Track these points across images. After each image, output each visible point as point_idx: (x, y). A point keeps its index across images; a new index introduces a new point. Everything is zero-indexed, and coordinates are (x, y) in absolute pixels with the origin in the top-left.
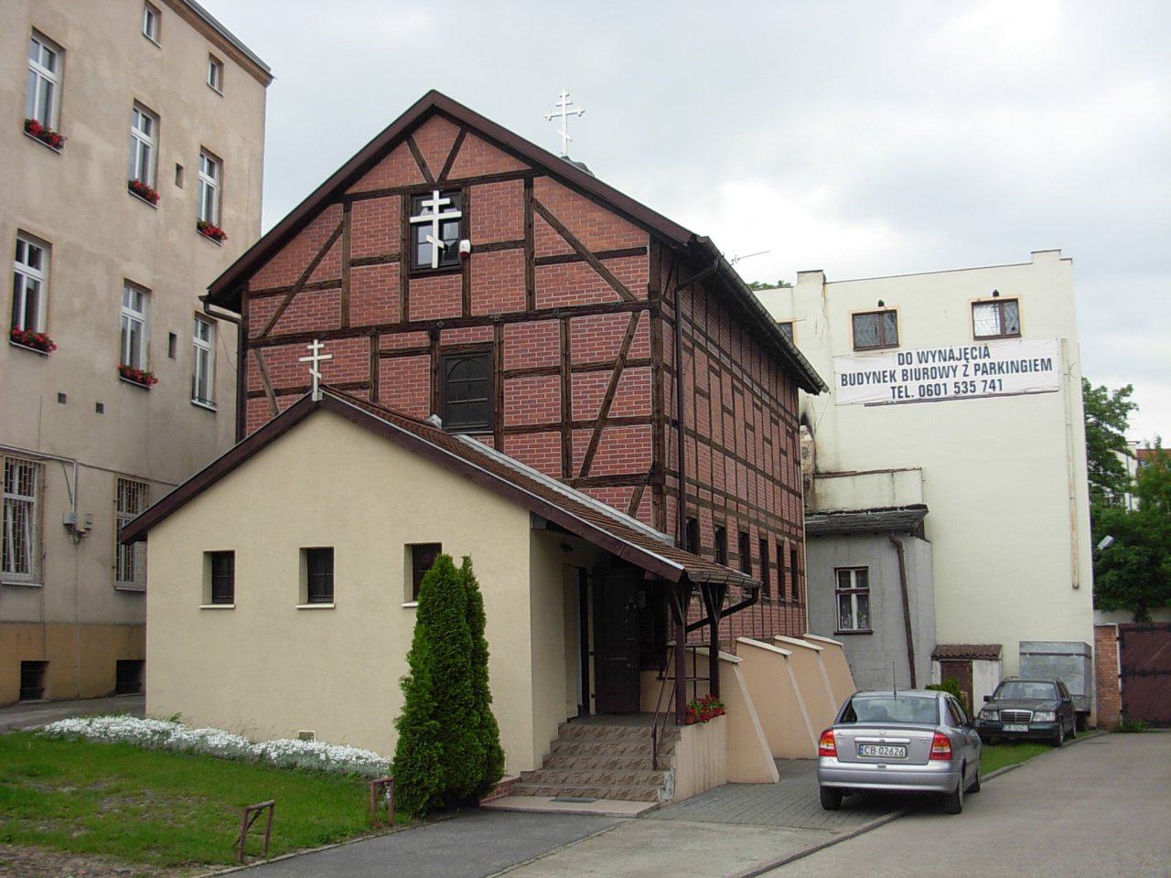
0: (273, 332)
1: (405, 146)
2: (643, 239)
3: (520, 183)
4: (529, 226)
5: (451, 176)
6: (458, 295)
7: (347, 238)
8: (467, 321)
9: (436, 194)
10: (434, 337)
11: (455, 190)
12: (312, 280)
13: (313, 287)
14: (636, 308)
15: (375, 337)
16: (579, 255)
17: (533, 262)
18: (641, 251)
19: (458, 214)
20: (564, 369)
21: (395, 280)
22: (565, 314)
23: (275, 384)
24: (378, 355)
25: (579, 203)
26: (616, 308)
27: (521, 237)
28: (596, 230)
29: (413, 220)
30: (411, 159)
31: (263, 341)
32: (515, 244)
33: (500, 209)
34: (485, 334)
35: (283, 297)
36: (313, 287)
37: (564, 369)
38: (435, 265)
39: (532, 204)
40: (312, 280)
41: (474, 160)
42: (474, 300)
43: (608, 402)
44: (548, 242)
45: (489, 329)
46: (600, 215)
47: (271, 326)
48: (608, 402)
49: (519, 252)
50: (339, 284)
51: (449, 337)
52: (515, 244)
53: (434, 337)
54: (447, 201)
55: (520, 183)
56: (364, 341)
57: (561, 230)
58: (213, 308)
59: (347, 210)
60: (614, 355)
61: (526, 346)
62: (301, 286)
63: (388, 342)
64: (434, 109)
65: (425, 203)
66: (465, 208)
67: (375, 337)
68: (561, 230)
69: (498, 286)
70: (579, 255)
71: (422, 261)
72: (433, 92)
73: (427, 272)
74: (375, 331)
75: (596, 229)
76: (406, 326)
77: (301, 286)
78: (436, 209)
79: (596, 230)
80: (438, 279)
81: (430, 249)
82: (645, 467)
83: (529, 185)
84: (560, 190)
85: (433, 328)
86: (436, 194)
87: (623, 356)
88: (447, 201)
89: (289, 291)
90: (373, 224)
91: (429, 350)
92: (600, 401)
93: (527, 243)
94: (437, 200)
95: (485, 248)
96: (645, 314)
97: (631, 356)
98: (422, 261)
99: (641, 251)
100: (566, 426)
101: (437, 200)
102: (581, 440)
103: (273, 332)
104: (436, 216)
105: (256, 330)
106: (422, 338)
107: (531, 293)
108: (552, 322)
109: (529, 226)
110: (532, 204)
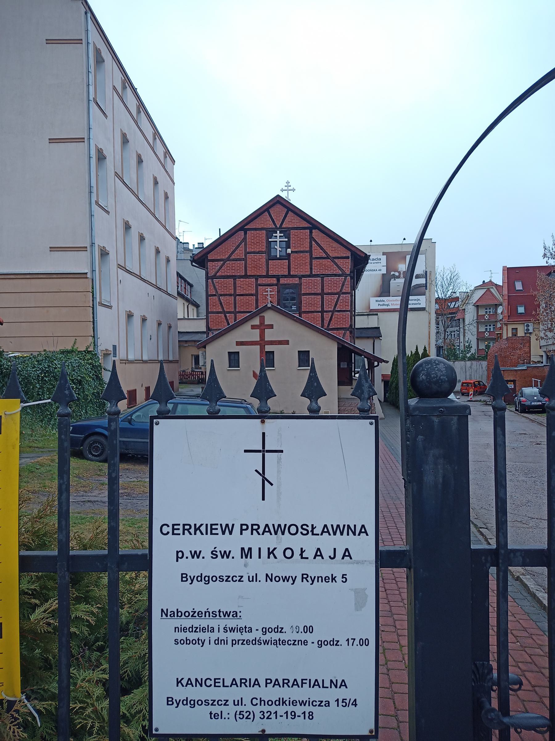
0: (218, 274)
1: (266, 213)
2: (349, 254)
3: (308, 231)
4: (311, 246)
5: (284, 226)
6: (286, 267)
7: (246, 245)
8: (289, 276)
9: (278, 232)
10: (278, 280)
11: (286, 232)
12: (233, 257)
13: (233, 260)
14: (346, 276)
15: (257, 280)
16: (328, 257)
17: (311, 258)
18: (348, 258)
19: (287, 240)
20: (322, 294)
21: (264, 260)
22: (323, 276)
23: (219, 292)
24: (257, 285)
25: (327, 240)
26: (339, 275)
27: (308, 249)
28: (334, 250)
29: (270, 240)
30: (269, 218)
31: (215, 277)
32: (306, 252)
33: (301, 239)
34: (296, 281)
35: (222, 262)
36: (233, 260)
37: (322, 294)
38: (278, 256)
39: (312, 238)
40: (233, 257)
41: (292, 221)
42: (292, 269)
43: (336, 305)
44: (317, 252)
45: (297, 279)
46: (335, 245)
47: (218, 272)
48: (336, 305)
49: (308, 254)
50: (243, 260)
51: (282, 281)
52: (306, 252)
53: (278, 280)
54: (282, 235)
55: (308, 231)
56: (253, 280)
57: (322, 248)
58: (194, 264)
59: (245, 234)
60: (338, 290)
61: (308, 285)
62: (228, 259)
63: (260, 281)
64: (278, 201)
65: (274, 235)
66: (288, 236)
67: (257, 280)
68: (322, 248)
69: (300, 266)
70: (328, 257)
71: (273, 254)
72: (278, 196)
73: (275, 258)
74: (257, 277)
75: (333, 249)
76: (267, 276)
77: (228, 259)
78: (278, 237)
79: (334, 250)
80: (280, 261)
81: (278, 250)
82: (348, 326)
83: (311, 232)
84: (321, 234)
85: (278, 278)
86: (278, 232)
87: (341, 291)
88: (282, 235)
89: (224, 261)
90: (256, 240)
91: (276, 285)
92: (333, 305)
93: (310, 252)
94: (278, 234)
95: (296, 252)
96: (349, 278)
97: (344, 291)
98: (273, 254)
99: (348, 258)
100: (322, 312)
101: (278, 234)
102: (327, 316)
103: (218, 274)
104: (278, 240)
105: (211, 273)
106: (274, 281)
107: (311, 269)
108: (318, 278)
109: (311, 246)
110: (312, 238)
